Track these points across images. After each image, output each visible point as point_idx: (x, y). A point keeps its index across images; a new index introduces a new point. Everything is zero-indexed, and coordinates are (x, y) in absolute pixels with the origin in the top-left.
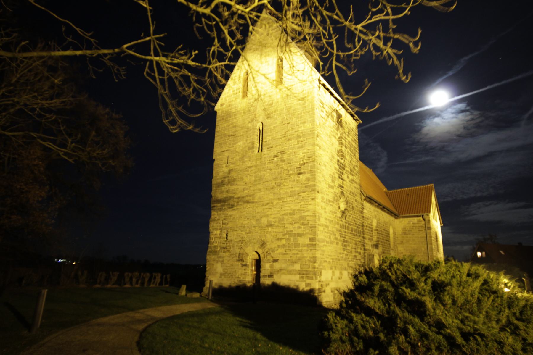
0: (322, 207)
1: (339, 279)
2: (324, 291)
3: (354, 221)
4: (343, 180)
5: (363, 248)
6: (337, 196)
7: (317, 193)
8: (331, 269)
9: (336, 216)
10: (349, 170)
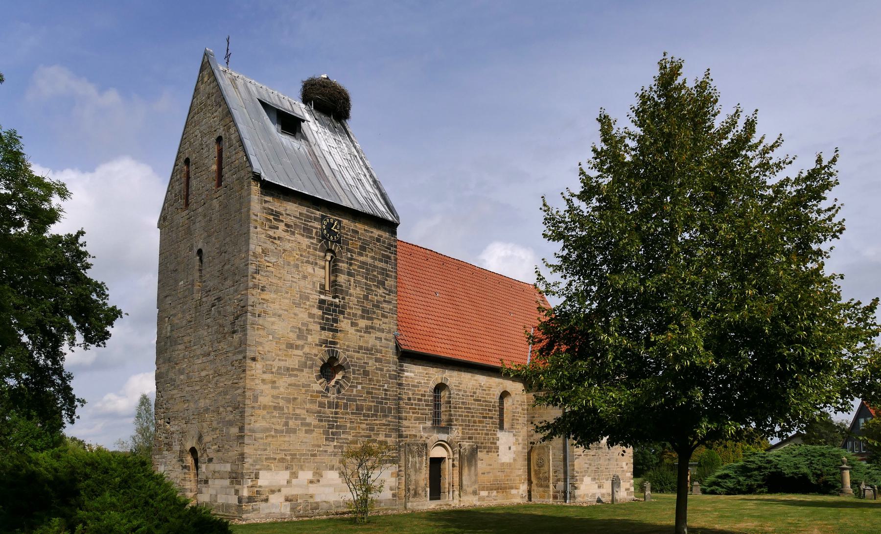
0: (263, 381)
1: (311, 482)
2: (266, 500)
3: (368, 393)
4: (336, 331)
5: (394, 435)
6: (311, 359)
7: (249, 361)
8: (287, 468)
9: (306, 391)
10: (359, 312)
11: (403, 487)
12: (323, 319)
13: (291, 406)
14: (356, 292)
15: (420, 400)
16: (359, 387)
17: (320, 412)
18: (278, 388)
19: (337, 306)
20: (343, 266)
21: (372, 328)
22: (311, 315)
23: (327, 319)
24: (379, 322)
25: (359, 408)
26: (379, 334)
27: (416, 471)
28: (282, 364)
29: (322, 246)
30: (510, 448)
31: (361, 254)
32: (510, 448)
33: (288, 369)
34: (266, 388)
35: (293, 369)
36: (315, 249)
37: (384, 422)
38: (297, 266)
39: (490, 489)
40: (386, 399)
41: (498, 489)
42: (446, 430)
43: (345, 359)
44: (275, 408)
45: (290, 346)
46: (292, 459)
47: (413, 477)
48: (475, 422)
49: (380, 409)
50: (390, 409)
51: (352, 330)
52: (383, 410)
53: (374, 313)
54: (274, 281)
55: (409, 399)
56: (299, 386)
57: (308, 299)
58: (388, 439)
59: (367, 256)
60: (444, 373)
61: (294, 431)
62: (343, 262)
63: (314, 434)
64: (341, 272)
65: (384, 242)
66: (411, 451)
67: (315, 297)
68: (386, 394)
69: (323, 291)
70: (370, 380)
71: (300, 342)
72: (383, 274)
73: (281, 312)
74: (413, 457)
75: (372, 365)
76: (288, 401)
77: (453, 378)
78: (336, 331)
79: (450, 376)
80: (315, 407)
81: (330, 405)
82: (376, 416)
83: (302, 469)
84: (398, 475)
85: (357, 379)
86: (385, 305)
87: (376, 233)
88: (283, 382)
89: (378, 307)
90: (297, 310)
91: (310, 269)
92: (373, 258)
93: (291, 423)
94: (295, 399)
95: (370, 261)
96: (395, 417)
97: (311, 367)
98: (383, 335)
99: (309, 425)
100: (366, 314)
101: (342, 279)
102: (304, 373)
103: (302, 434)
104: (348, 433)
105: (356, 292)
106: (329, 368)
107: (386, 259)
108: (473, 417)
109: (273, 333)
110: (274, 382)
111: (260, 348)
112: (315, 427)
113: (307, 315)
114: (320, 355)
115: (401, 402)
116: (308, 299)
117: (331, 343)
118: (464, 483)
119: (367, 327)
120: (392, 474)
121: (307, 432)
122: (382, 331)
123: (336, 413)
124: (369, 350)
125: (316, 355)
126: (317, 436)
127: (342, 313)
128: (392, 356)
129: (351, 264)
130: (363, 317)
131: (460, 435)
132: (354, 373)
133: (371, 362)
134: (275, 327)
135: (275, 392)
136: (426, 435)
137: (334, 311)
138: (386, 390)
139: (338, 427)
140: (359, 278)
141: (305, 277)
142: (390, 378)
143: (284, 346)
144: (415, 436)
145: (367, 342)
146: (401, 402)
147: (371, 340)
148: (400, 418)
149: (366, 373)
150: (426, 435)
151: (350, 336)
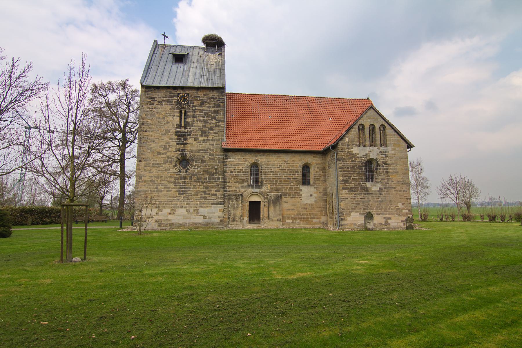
0: (145, 170)
3: (204, 171)
5: (221, 190)
6: (171, 158)
10: (200, 134)
11: (227, 216)
12: (178, 139)
13: (159, 180)
14: (198, 124)
15: (238, 172)
16: (199, 169)
17: (174, 182)
18: (152, 172)
19: (186, 132)
20: (190, 114)
21: (208, 140)
22: (171, 139)
23: (180, 139)
24: (212, 137)
25: (199, 179)
26: (212, 142)
27: (234, 208)
28: (155, 162)
29: (178, 107)
30: (311, 195)
31: (202, 107)
32: (311, 195)
33: (158, 164)
34: (146, 173)
35: (160, 164)
36: (174, 109)
37: (215, 184)
38: (164, 118)
39: (294, 218)
40: (216, 173)
41: (301, 218)
42: (258, 187)
43: (191, 156)
44: (151, 181)
45: (159, 154)
46: (159, 204)
47: (232, 211)
48: (281, 181)
49: (212, 178)
50: (219, 178)
51: (195, 142)
52: (213, 179)
53: (209, 132)
54: (151, 127)
55: (232, 172)
56: (163, 171)
57: (169, 132)
58: (217, 193)
59: (205, 106)
60: (256, 156)
61: (161, 191)
62: (190, 112)
63: (172, 192)
64: (189, 116)
65: (216, 98)
66: (231, 199)
67: (174, 130)
68: (216, 171)
69: (180, 126)
70: (206, 165)
71: (165, 151)
72: (215, 113)
73: (154, 139)
74: (232, 201)
75: (207, 157)
76: (158, 178)
77: (262, 160)
78: (186, 144)
79: (261, 159)
80: (173, 180)
81: (181, 178)
82: (210, 182)
83: (164, 207)
84: (224, 211)
85: (198, 165)
86: (216, 128)
87: (211, 95)
88: (155, 170)
89: (211, 129)
90: (163, 138)
91: (171, 118)
92: (209, 107)
93: (159, 188)
94: (161, 177)
95: (206, 108)
96: (222, 182)
97: (170, 162)
98: (215, 143)
99: (169, 188)
100: (203, 133)
101: (189, 120)
102: (167, 165)
103: (165, 192)
104: (192, 191)
105: (198, 124)
106: (184, 161)
107: (218, 106)
108: (279, 179)
109: (150, 149)
110: (151, 170)
111: (144, 156)
112: (172, 188)
113: (170, 139)
114: (177, 155)
115: (226, 174)
116: (169, 132)
117: (182, 150)
118: (270, 215)
119: (204, 140)
120: (220, 210)
121: (167, 191)
122: (214, 140)
123: (185, 182)
124: (205, 151)
125: (173, 156)
126: (174, 192)
127: (189, 135)
128: (222, 153)
129: (195, 112)
130: (202, 136)
131: (269, 189)
132: (196, 162)
133: (206, 156)
134: (151, 146)
135: (151, 175)
136: (243, 190)
137: (184, 135)
138: (216, 169)
139: (185, 188)
140: (200, 118)
141: (168, 122)
142: (219, 162)
143: (156, 154)
144: (236, 191)
145: (205, 147)
146: (226, 174)
147: (207, 145)
148: (225, 182)
149: (203, 162)
150: (243, 190)
151: (193, 145)
